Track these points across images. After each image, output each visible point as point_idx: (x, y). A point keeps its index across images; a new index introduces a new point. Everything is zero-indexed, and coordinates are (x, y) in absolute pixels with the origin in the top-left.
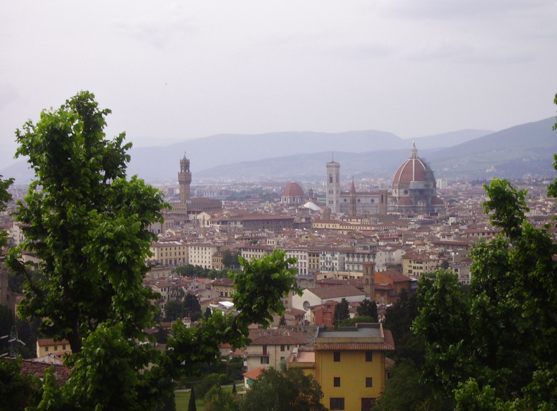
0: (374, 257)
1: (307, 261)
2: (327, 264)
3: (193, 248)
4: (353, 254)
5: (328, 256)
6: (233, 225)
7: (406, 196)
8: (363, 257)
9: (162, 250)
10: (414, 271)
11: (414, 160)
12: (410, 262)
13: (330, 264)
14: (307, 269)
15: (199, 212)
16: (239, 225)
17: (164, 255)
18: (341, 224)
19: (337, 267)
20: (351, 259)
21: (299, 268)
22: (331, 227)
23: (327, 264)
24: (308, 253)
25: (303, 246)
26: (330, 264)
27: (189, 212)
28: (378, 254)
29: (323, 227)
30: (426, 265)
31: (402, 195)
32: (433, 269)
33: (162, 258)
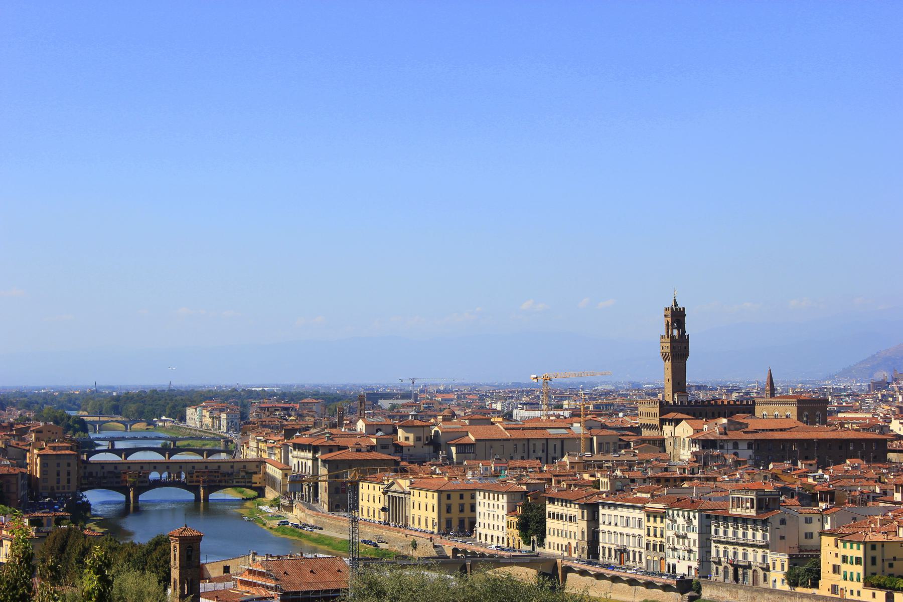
1: (643, 533)
2: (678, 543)
3: (482, 494)
9: (449, 497)
10: (844, 567)
13: (684, 543)
14: (643, 551)
15: (677, 422)
16: (745, 453)
17: (455, 509)
19: (696, 549)
21: (631, 549)
23: (678, 543)
25: (643, 495)
26: (684, 543)
27: (663, 422)
30: (871, 553)
33: (449, 515)
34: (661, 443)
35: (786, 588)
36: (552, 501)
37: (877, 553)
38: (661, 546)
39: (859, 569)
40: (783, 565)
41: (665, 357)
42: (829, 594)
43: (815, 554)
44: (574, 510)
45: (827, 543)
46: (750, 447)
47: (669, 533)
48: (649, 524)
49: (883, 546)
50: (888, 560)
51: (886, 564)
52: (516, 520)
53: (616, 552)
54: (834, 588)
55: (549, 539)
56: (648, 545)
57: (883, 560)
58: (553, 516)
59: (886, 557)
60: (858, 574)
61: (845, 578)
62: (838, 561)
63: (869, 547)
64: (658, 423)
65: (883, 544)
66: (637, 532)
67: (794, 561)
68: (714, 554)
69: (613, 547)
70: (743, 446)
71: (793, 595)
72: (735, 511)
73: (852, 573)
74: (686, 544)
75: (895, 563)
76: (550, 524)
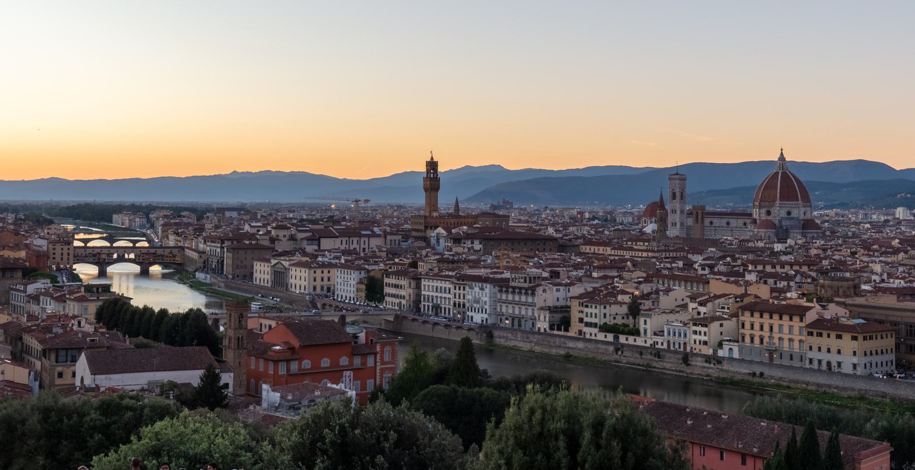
0: (533, 294)
4: (508, 287)
5: (477, 289)
6: (469, 244)
7: (769, 218)
8: (520, 293)
16: (477, 246)
18: (614, 249)
19: (487, 307)
20: (504, 297)
22: (601, 252)
24: (453, 283)
25: (450, 273)
27: (426, 227)
28: (539, 290)
30: (603, 311)
32: (619, 318)
34: (426, 239)
35: (547, 329)
36: (388, 276)
38: (464, 305)
41: (426, 190)
43: (566, 309)
44: (404, 282)
46: (480, 243)
47: (469, 297)
52: (364, 287)
54: (580, 332)
55: (387, 299)
56: (455, 304)
58: (389, 285)
62: (582, 316)
63: (602, 307)
64: (423, 228)
66: (448, 296)
68: (499, 310)
69: (431, 304)
70: (477, 242)
72: (512, 284)
76: (387, 290)
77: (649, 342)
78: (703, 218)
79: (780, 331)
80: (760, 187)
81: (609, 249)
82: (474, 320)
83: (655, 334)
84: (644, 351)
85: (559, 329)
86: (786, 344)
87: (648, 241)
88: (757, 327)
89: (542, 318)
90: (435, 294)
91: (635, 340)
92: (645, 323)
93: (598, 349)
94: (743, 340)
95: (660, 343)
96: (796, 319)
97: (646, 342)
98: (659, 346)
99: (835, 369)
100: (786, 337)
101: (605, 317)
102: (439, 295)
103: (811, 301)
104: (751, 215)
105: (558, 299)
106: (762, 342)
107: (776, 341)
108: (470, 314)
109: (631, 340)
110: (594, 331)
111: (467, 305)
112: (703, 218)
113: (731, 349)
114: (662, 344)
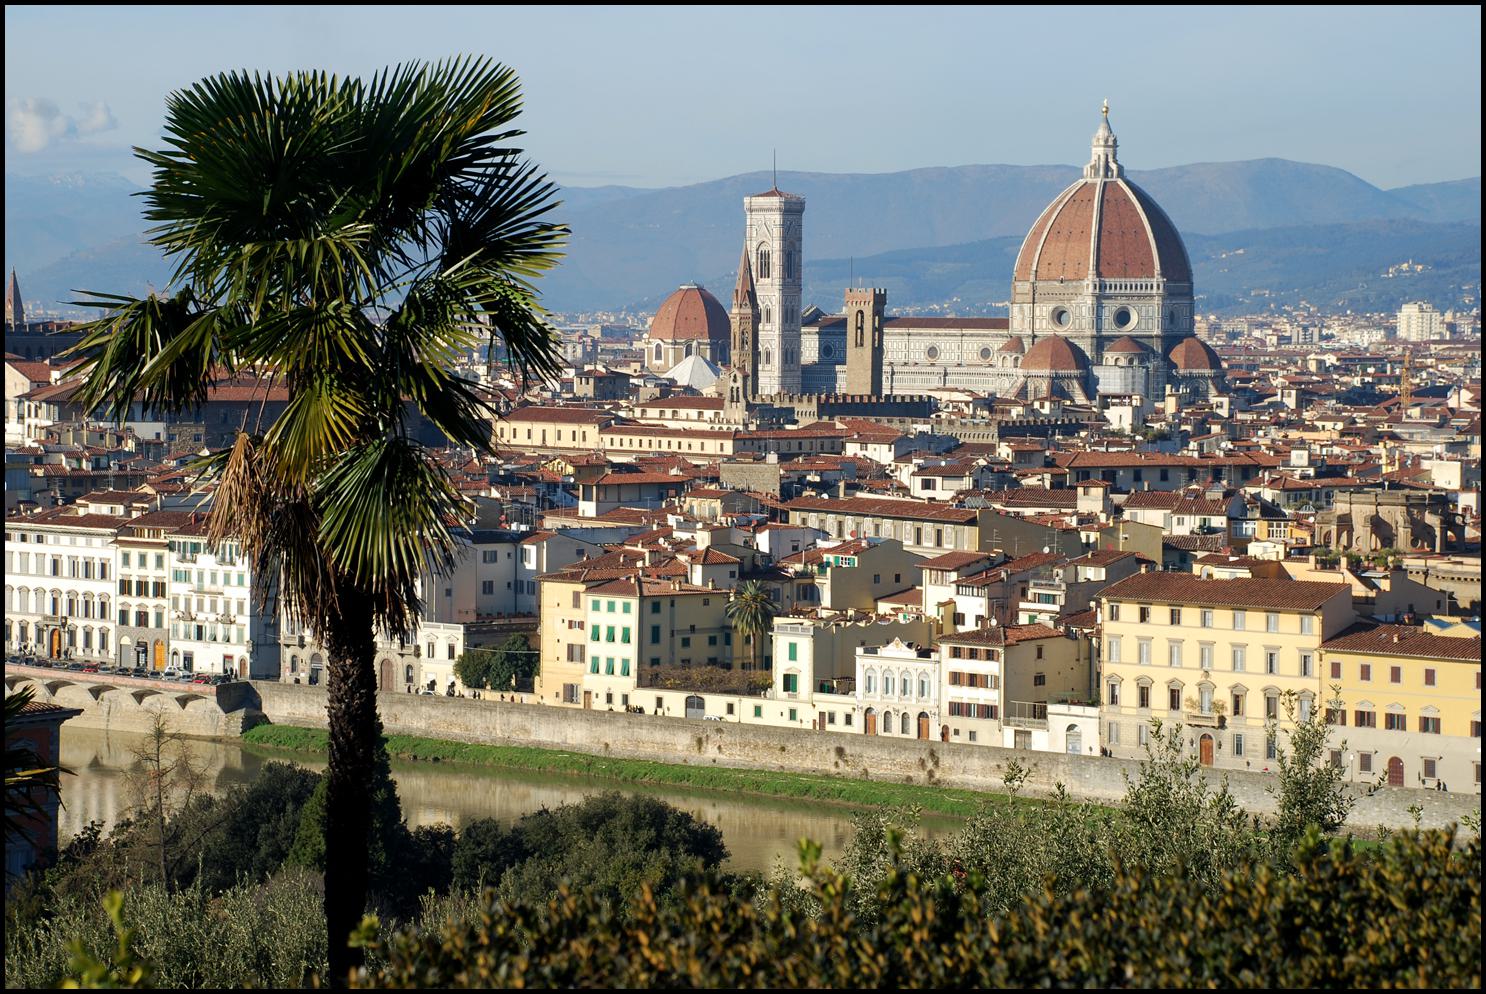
1: (111, 588)
2: (200, 608)
7: (1062, 332)
11: (1099, 181)
12: (576, 603)
13: (213, 608)
18: (605, 428)
21: (79, 623)
23: (200, 608)
26: (213, 608)
29: (537, 440)
31: (1045, 328)
32: (700, 641)
37: (662, 620)
39: (630, 652)
40: (451, 649)
42: (559, 702)
43: (527, 621)
45: (557, 600)
47: (174, 588)
48: (126, 571)
49: (672, 605)
50: (680, 632)
51: (678, 639)
53: (40, 631)
54: (570, 692)
57: (672, 634)
59: (677, 627)
60: (626, 662)
61: (596, 670)
65: (672, 599)
67: (476, 639)
69: (32, 621)
71: (490, 707)
73: (610, 662)
74: (221, 609)
75: (694, 638)
77: (807, 718)
78: (878, 331)
79: (1237, 663)
80: (1037, 234)
81: (592, 430)
82: (200, 665)
83: (822, 687)
84: (790, 746)
85: (503, 686)
86: (1255, 706)
87: (716, 403)
88: (1159, 651)
89: (442, 651)
90: (49, 583)
91: (758, 711)
92: (793, 656)
93: (638, 742)
94: (1114, 700)
95: (840, 719)
96: (1289, 621)
97: (793, 714)
98: (839, 726)
99: (1411, 780)
100: (1255, 686)
101: (656, 639)
102: (64, 584)
103: (1329, 564)
104: (1004, 324)
105: (488, 587)
106: (1174, 703)
107: (1224, 696)
108: (181, 646)
109: (745, 706)
110: (625, 685)
111: (169, 617)
112: (878, 331)
113: (1071, 727)
114: (848, 720)
